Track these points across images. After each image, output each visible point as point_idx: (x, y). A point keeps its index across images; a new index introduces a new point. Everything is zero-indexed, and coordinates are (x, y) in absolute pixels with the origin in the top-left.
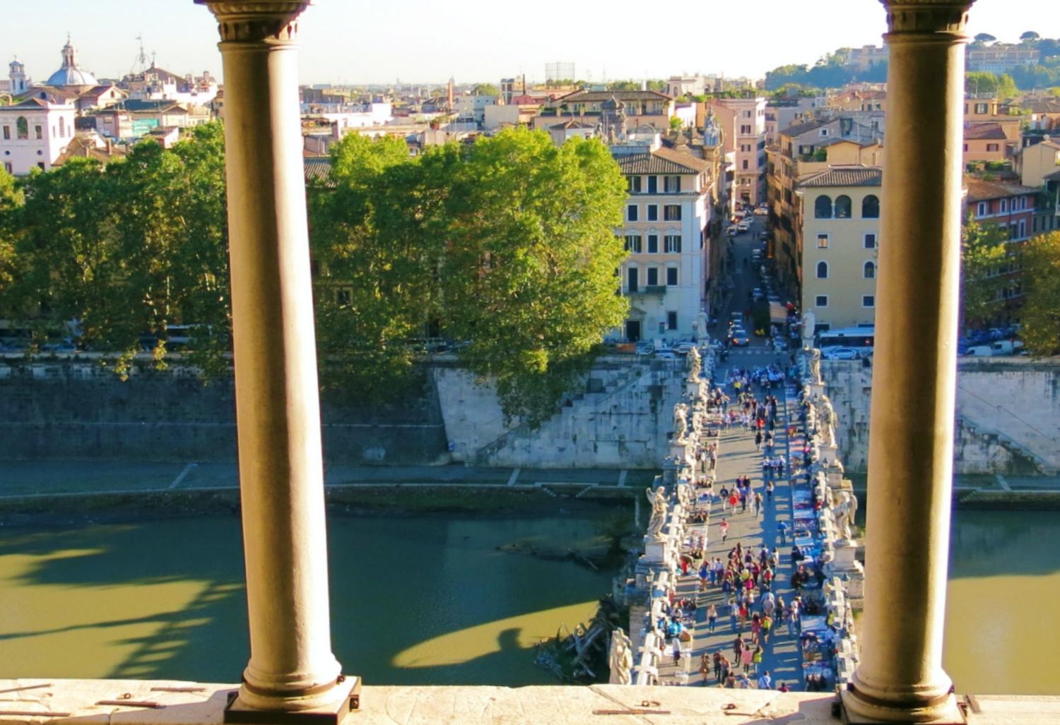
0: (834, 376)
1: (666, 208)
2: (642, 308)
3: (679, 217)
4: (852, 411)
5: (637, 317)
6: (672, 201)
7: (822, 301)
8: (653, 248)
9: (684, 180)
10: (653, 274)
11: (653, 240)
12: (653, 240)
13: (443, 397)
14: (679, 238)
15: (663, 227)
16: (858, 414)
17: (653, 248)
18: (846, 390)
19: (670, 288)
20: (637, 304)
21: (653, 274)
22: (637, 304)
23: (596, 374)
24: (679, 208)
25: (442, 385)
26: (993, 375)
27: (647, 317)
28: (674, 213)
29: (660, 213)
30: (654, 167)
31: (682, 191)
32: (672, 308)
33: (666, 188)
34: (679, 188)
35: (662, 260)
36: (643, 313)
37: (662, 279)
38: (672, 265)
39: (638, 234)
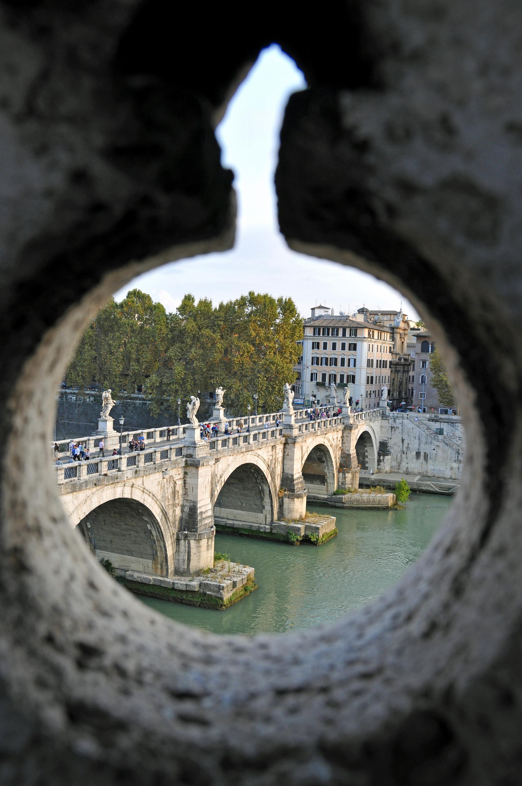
0: (394, 421)
1: (350, 344)
3: (356, 350)
4: (403, 440)
8: (343, 364)
9: (359, 331)
11: (343, 360)
12: (343, 360)
14: (355, 360)
15: (347, 354)
16: (406, 442)
17: (343, 364)
18: (400, 428)
19: (350, 384)
21: (342, 376)
24: (355, 345)
28: (353, 347)
30: (346, 325)
31: (358, 336)
33: (350, 335)
34: (356, 336)
35: (347, 371)
39: (336, 357)
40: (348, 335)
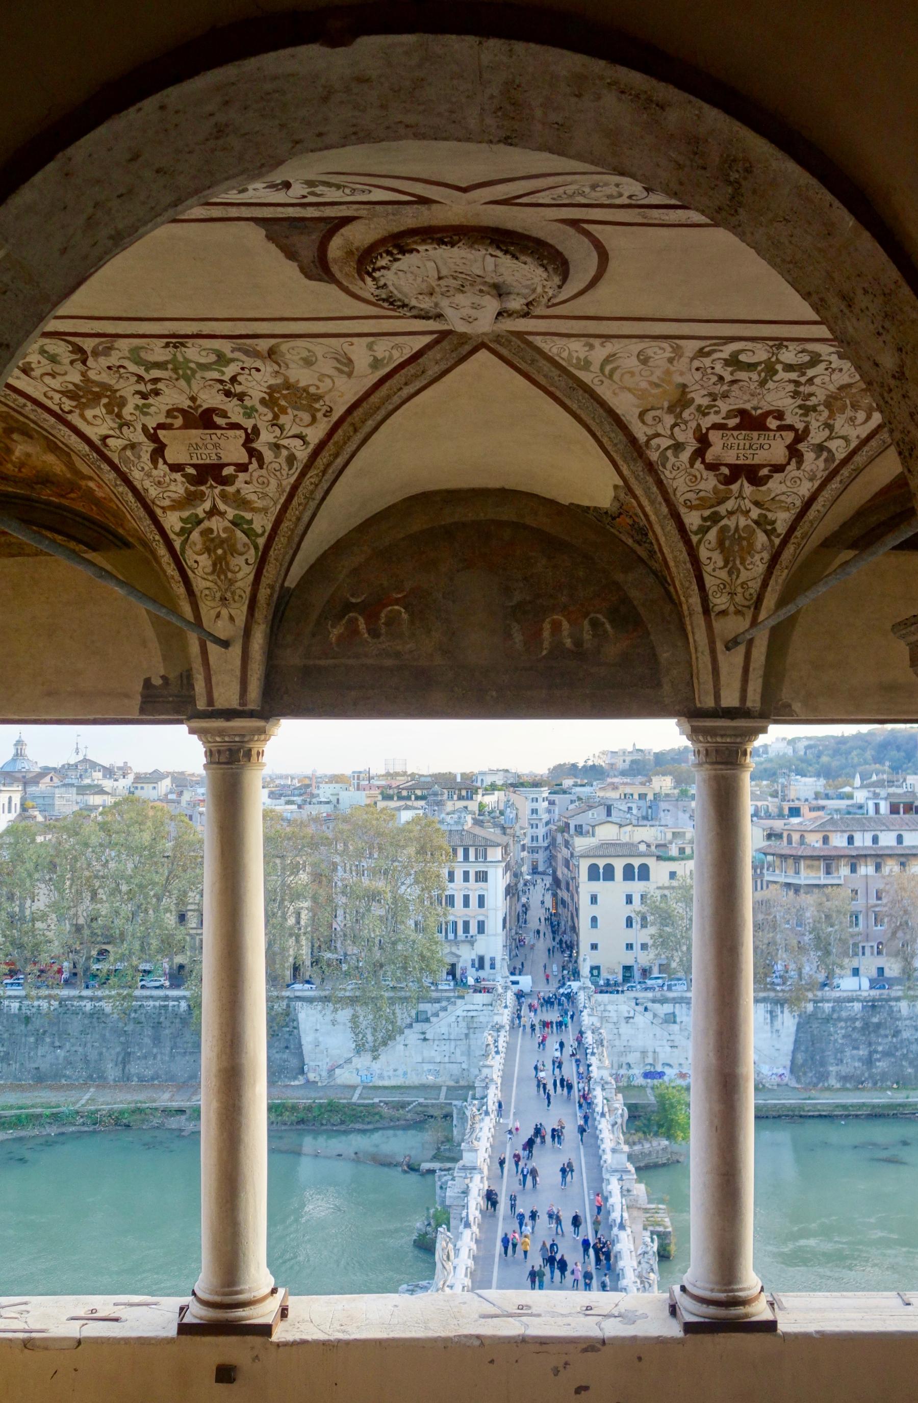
2: (458, 952)
5: (454, 960)
6: (481, 867)
7: (594, 947)
10: (466, 925)
13: (302, 1027)
15: (474, 889)
19: (479, 937)
20: (454, 949)
22: (454, 949)
23: (422, 1007)
25: (302, 1016)
27: (461, 959)
28: (482, 877)
29: (472, 877)
32: (481, 953)
36: (458, 956)
37: (473, 929)
38: (481, 918)
40: (472, 857)
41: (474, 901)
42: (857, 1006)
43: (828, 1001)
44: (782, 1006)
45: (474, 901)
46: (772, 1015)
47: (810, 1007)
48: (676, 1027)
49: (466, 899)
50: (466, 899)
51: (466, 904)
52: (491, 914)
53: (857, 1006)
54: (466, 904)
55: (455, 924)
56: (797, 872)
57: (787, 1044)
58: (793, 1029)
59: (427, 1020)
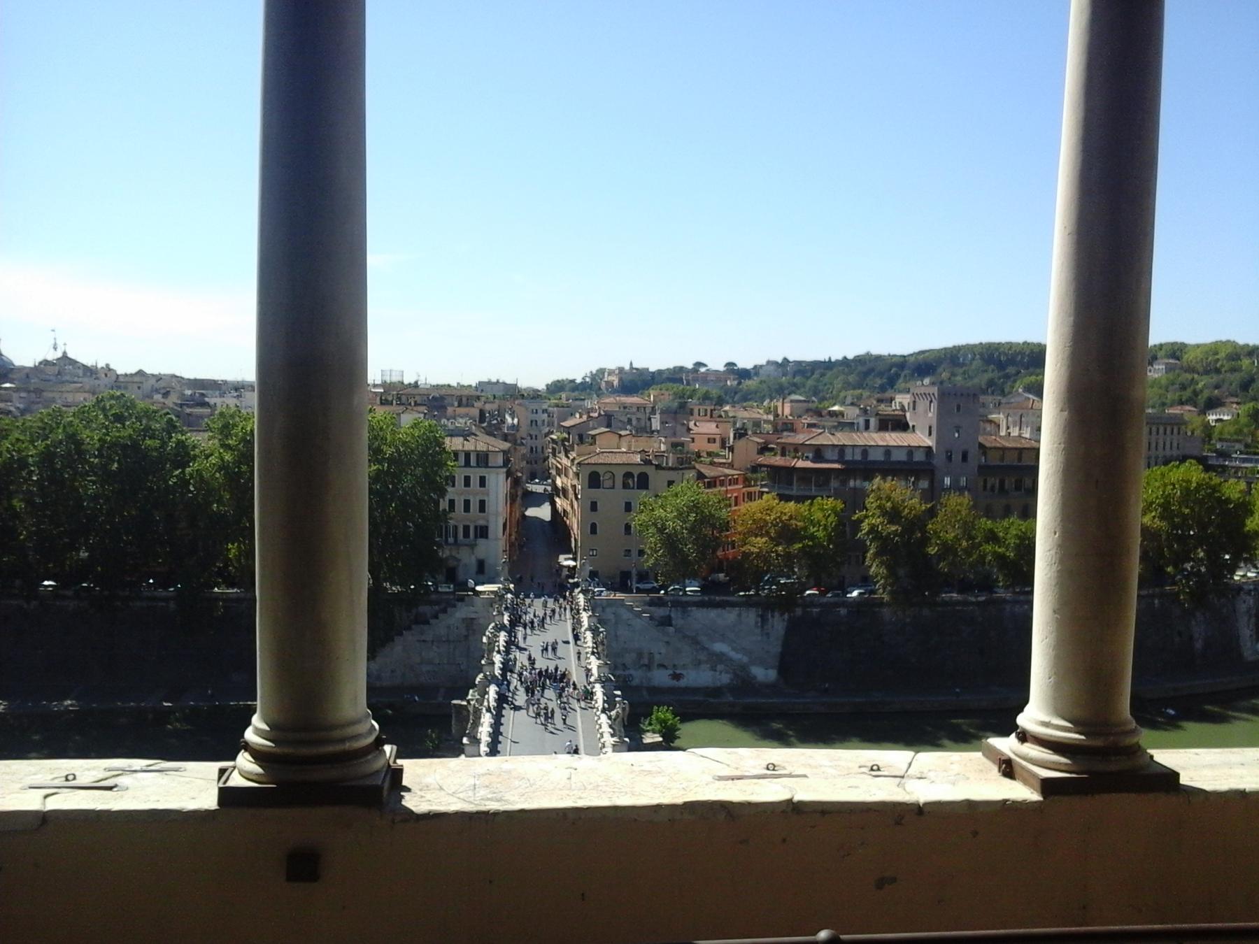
19: (481, 541)
26: (719, 610)
41: (474, 506)
42: (843, 611)
43: (815, 606)
44: (773, 611)
45: (474, 506)
46: (764, 619)
47: (799, 611)
48: (671, 629)
49: (467, 503)
50: (467, 503)
51: (467, 509)
52: (492, 519)
53: (843, 611)
54: (467, 509)
55: (456, 527)
56: (791, 484)
57: (776, 648)
58: (782, 632)
59: (427, 623)
